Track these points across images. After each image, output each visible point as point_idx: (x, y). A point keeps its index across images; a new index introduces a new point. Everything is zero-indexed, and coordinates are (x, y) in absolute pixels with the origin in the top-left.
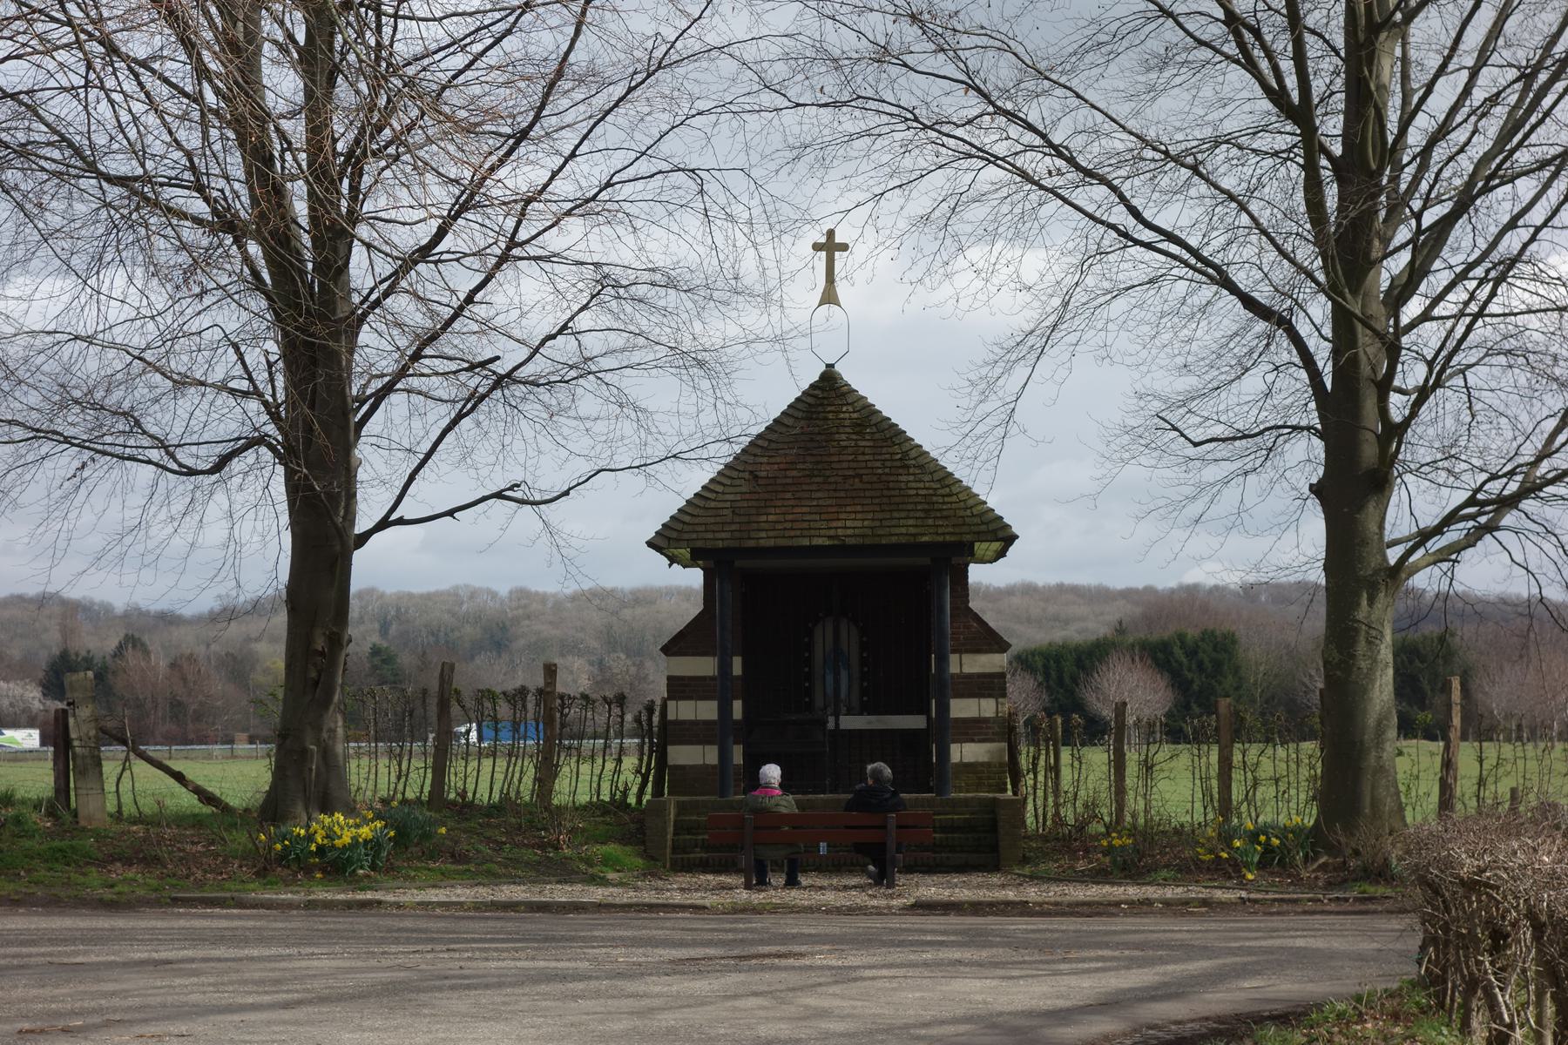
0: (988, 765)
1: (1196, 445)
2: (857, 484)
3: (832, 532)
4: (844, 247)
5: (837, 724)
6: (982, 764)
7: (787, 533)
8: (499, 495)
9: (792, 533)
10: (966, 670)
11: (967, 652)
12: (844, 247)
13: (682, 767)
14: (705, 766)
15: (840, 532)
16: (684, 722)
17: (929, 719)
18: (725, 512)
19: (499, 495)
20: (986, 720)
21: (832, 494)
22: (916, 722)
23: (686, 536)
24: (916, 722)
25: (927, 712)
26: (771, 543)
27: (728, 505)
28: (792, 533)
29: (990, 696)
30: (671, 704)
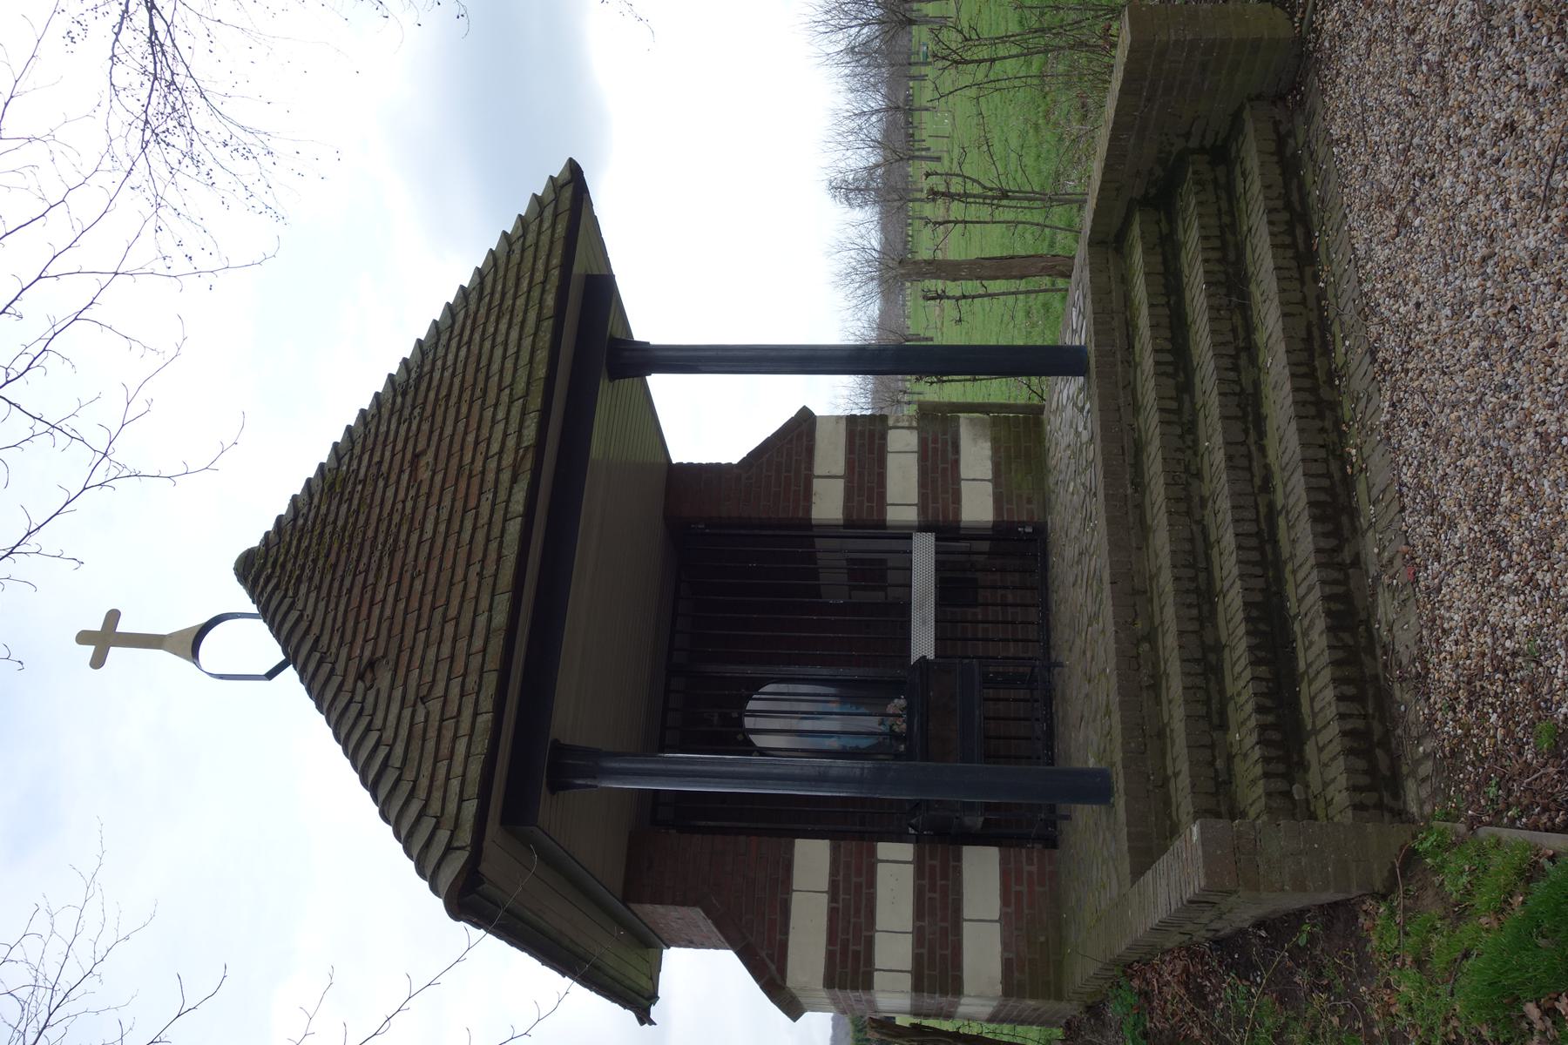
0: (996, 442)
2: (429, 457)
3: (506, 476)
6: (995, 450)
7: (490, 569)
9: (493, 555)
10: (840, 468)
13: (1007, 966)
14: (1005, 919)
15: (508, 460)
16: (917, 959)
17: (923, 528)
18: (420, 717)
20: (923, 442)
21: (434, 499)
23: (452, 807)
24: (924, 550)
26: (503, 602)
27: (407, 713)
28: (493, 555)
29: (884, 437)
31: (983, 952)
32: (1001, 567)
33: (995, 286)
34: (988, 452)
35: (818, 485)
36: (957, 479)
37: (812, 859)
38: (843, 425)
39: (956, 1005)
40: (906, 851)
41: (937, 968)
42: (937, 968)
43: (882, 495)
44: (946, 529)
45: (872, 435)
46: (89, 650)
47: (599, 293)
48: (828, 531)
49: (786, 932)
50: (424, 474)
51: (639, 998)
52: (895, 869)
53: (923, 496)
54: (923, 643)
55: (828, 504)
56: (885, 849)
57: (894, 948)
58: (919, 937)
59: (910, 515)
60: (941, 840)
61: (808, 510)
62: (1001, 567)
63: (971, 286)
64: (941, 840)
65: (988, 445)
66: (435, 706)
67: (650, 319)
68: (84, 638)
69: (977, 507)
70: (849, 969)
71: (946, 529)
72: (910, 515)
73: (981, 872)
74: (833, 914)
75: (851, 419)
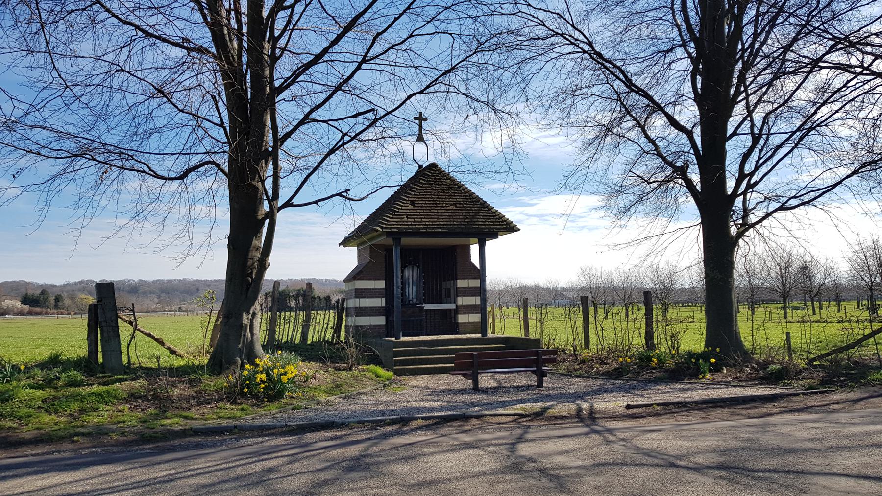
4: (426, 119)
8: (340, 195)
12: (426, 119)
19: (340, 195)
24: (452, 306)
31: (364, 321)
32: (447, 322)
33: (522, 322)
36: (469, 313)
37: (381, 284)
39: (352, 316)
40: (384, 304)
41: (361, 312)
42: (361, 312)
44: (457, 311)
47: (494, 235)
48: (455, 284)
50: (451, 207)
51: (345, 243)
52: (380, 302)
54: (428, 307)
55: (461, 283)
56: (384, 300)
57: (364, 302)
58: (367, 307)
59: (459, 303)
60: (386, 311)
62: (447, 322)
63: (522, 316)
64: (386, 311)
66: (406, 219)
67: (490, 244)
68: (421, 114)
69: (462, 318)
70: (360, 293)
71: (457, 311)
72: (459, 303)
73: (381, 321)
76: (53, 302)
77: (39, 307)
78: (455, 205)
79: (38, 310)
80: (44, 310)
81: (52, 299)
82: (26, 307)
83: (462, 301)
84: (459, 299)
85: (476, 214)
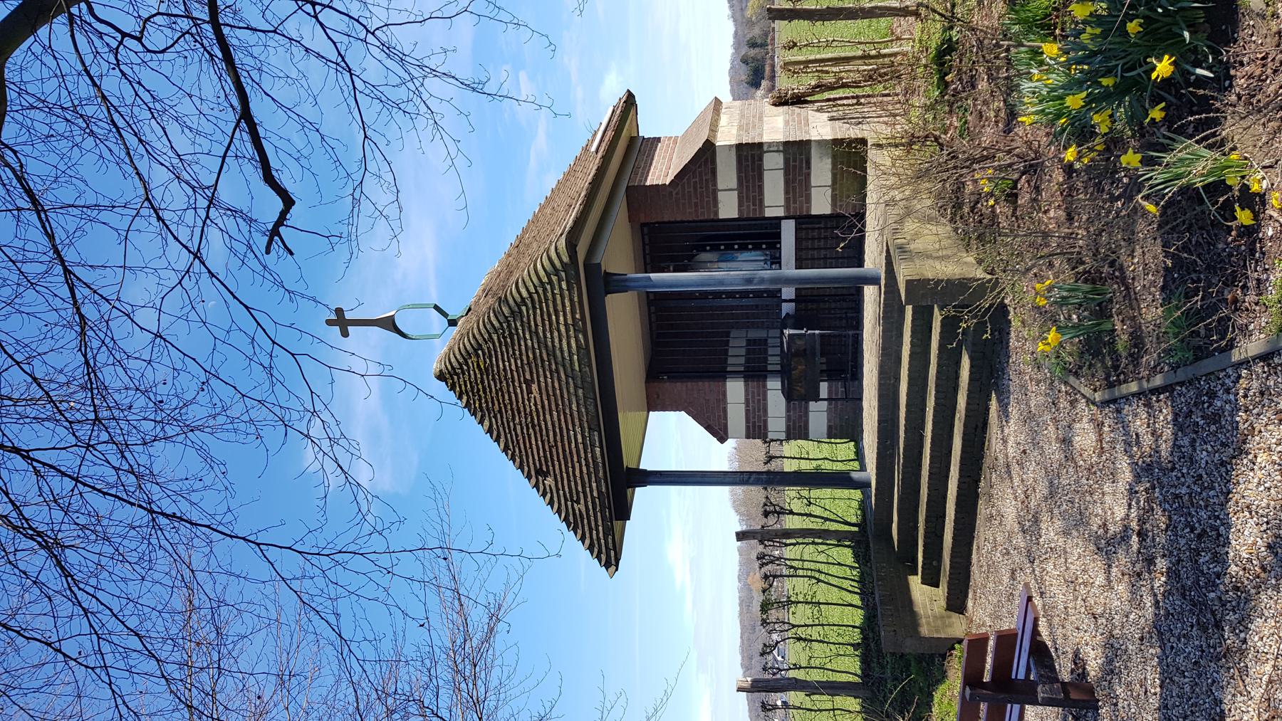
0: (834, 157)
1: (288, 202)
5: (790, 301)
10: (734, 183)
11: (715, 184)
13: (830, 428)
16: (788, 427)
17: (786, 218)
20: (786, 161)
22: (788, 231)
24: (788, 231)
25: (778, 220)
29: (761, 159)
30: (771, 436)
34: (830, 166)
35: (721, 195)
36: (808, 186)
38: (734, 150)
43: (761, 201)
45: (753, 156)
46: (334, 317)
49: (726, 418)
53: (787, 200)
58: (788, 418)
61: (716, 213)
65: (830, 161)
72: (780, 212)
74: (747, 412)
75: (740, 147)
76: (757, 50)
77: (763, 66)
78: (528, 383)
79: (767, 69)
80: (769, 62)
81: (752, 52)
82: (764, 83)
83: (774, 202)
84: (769, 213)
85: (542, 343)
